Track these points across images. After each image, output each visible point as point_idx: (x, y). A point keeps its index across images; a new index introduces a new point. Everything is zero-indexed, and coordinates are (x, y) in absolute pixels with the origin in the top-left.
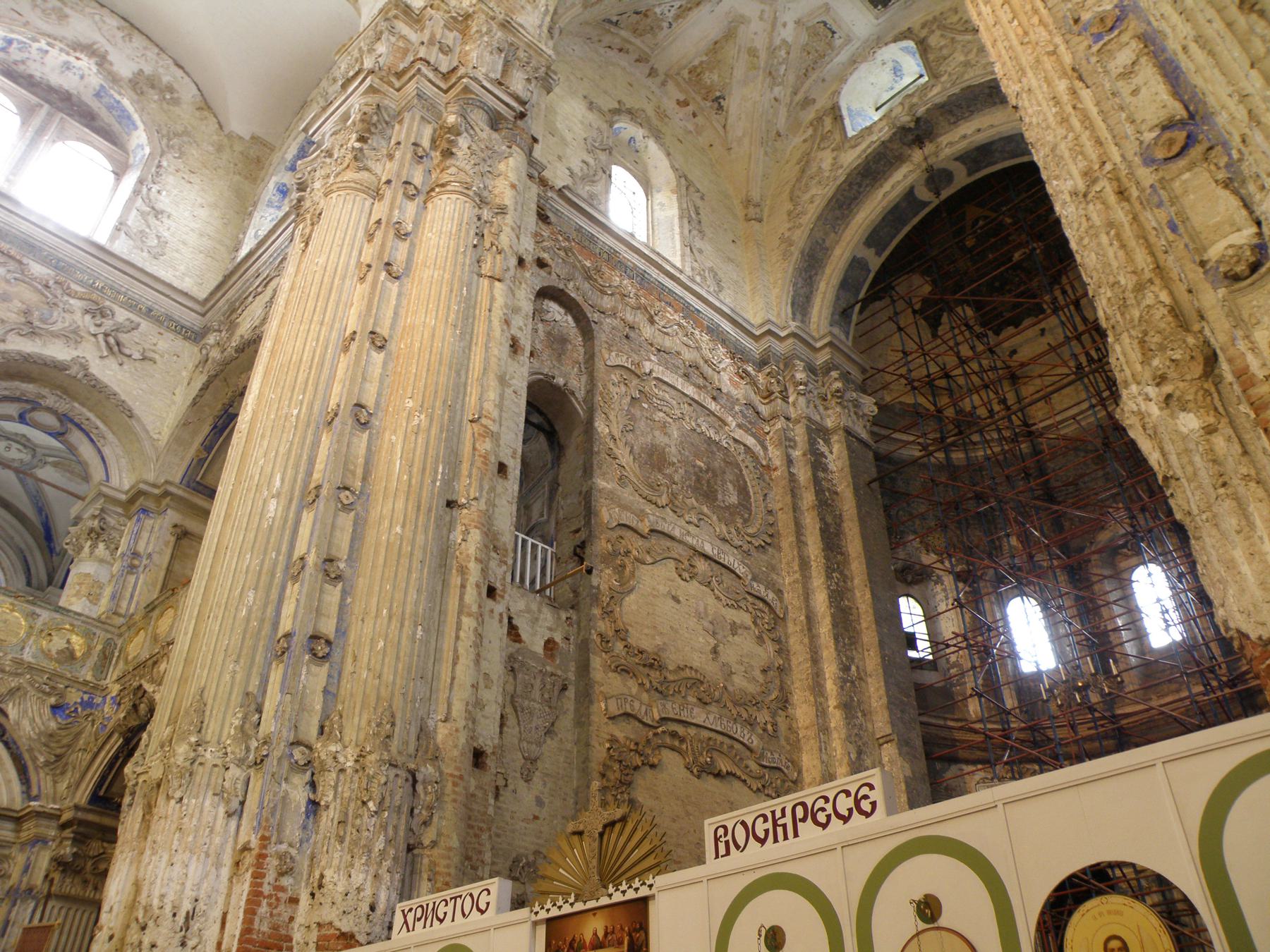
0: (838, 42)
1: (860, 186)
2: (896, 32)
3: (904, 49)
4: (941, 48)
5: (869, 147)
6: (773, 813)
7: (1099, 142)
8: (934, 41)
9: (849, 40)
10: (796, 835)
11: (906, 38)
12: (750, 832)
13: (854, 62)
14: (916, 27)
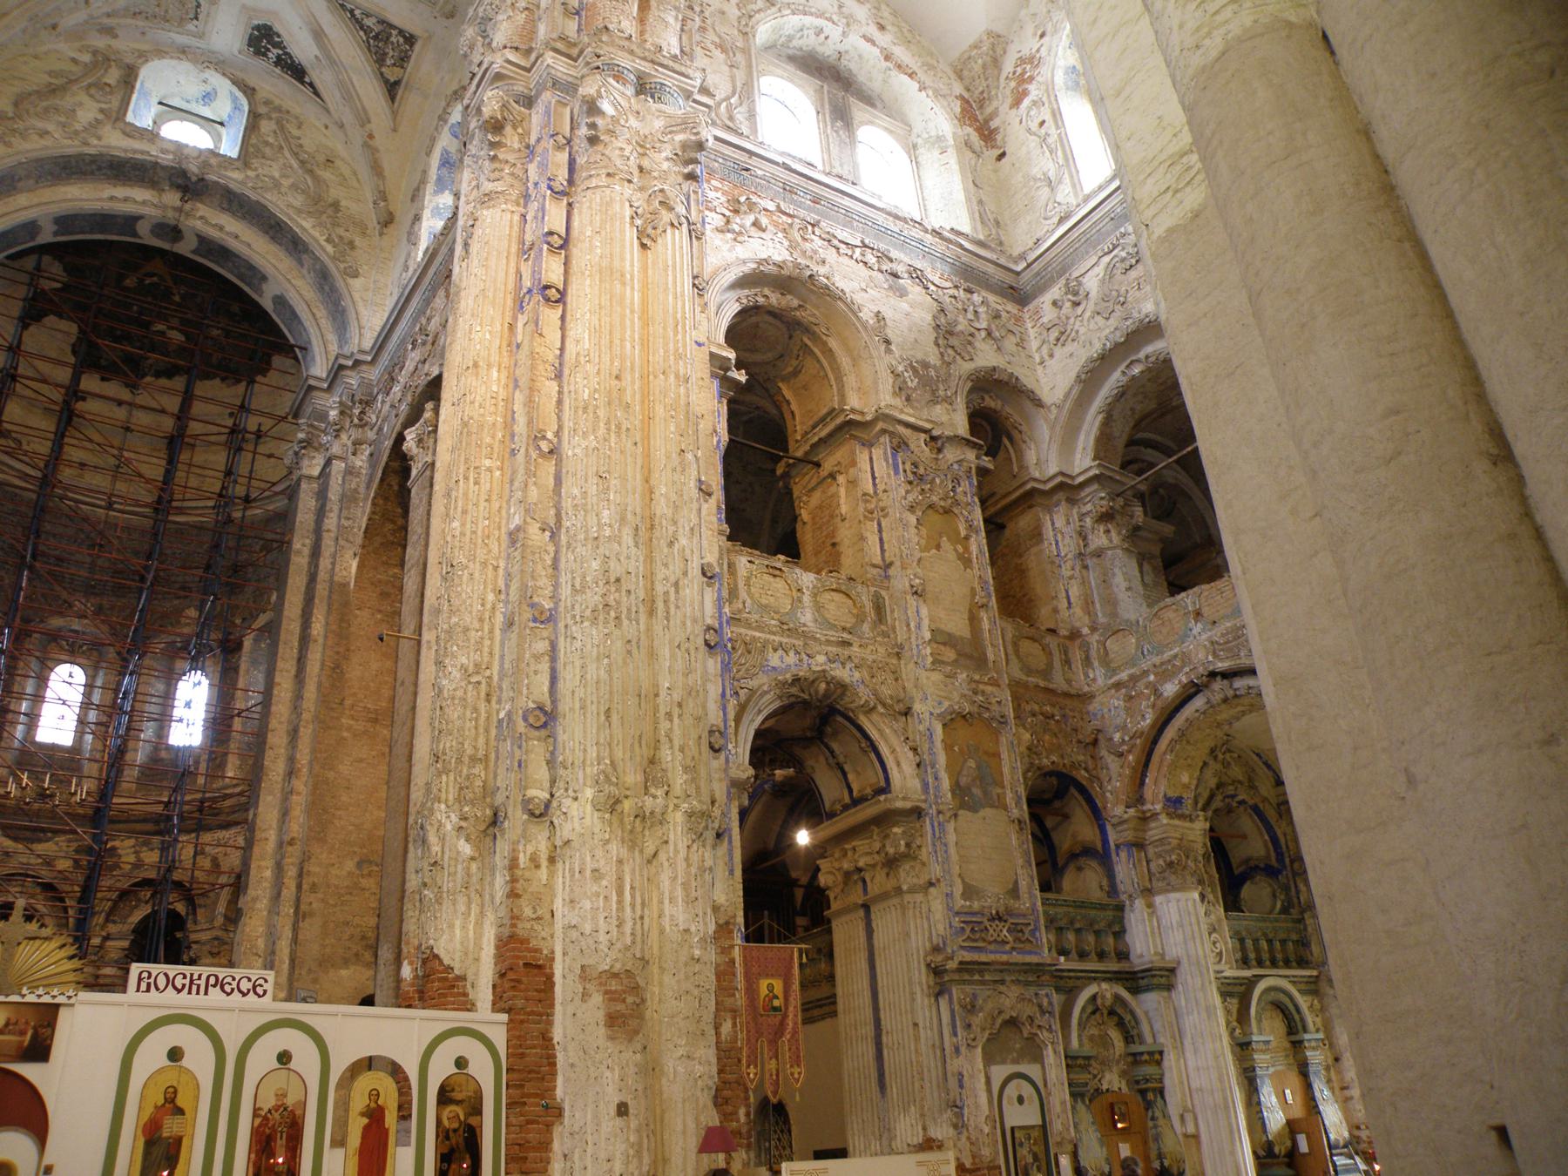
0: (191, 27)
1: (100, 169)
2: (240, 75)
3: (235, 99)
4: (267, 143)
5: (142, 152)
6: (192, 975)
7: (491, 654)
8: (266, 127)
9: (201, 36)
10: (206, 993)
11: (245, 93)
12: (170, 982)
13: (183, 52)
14: (261, 95)
